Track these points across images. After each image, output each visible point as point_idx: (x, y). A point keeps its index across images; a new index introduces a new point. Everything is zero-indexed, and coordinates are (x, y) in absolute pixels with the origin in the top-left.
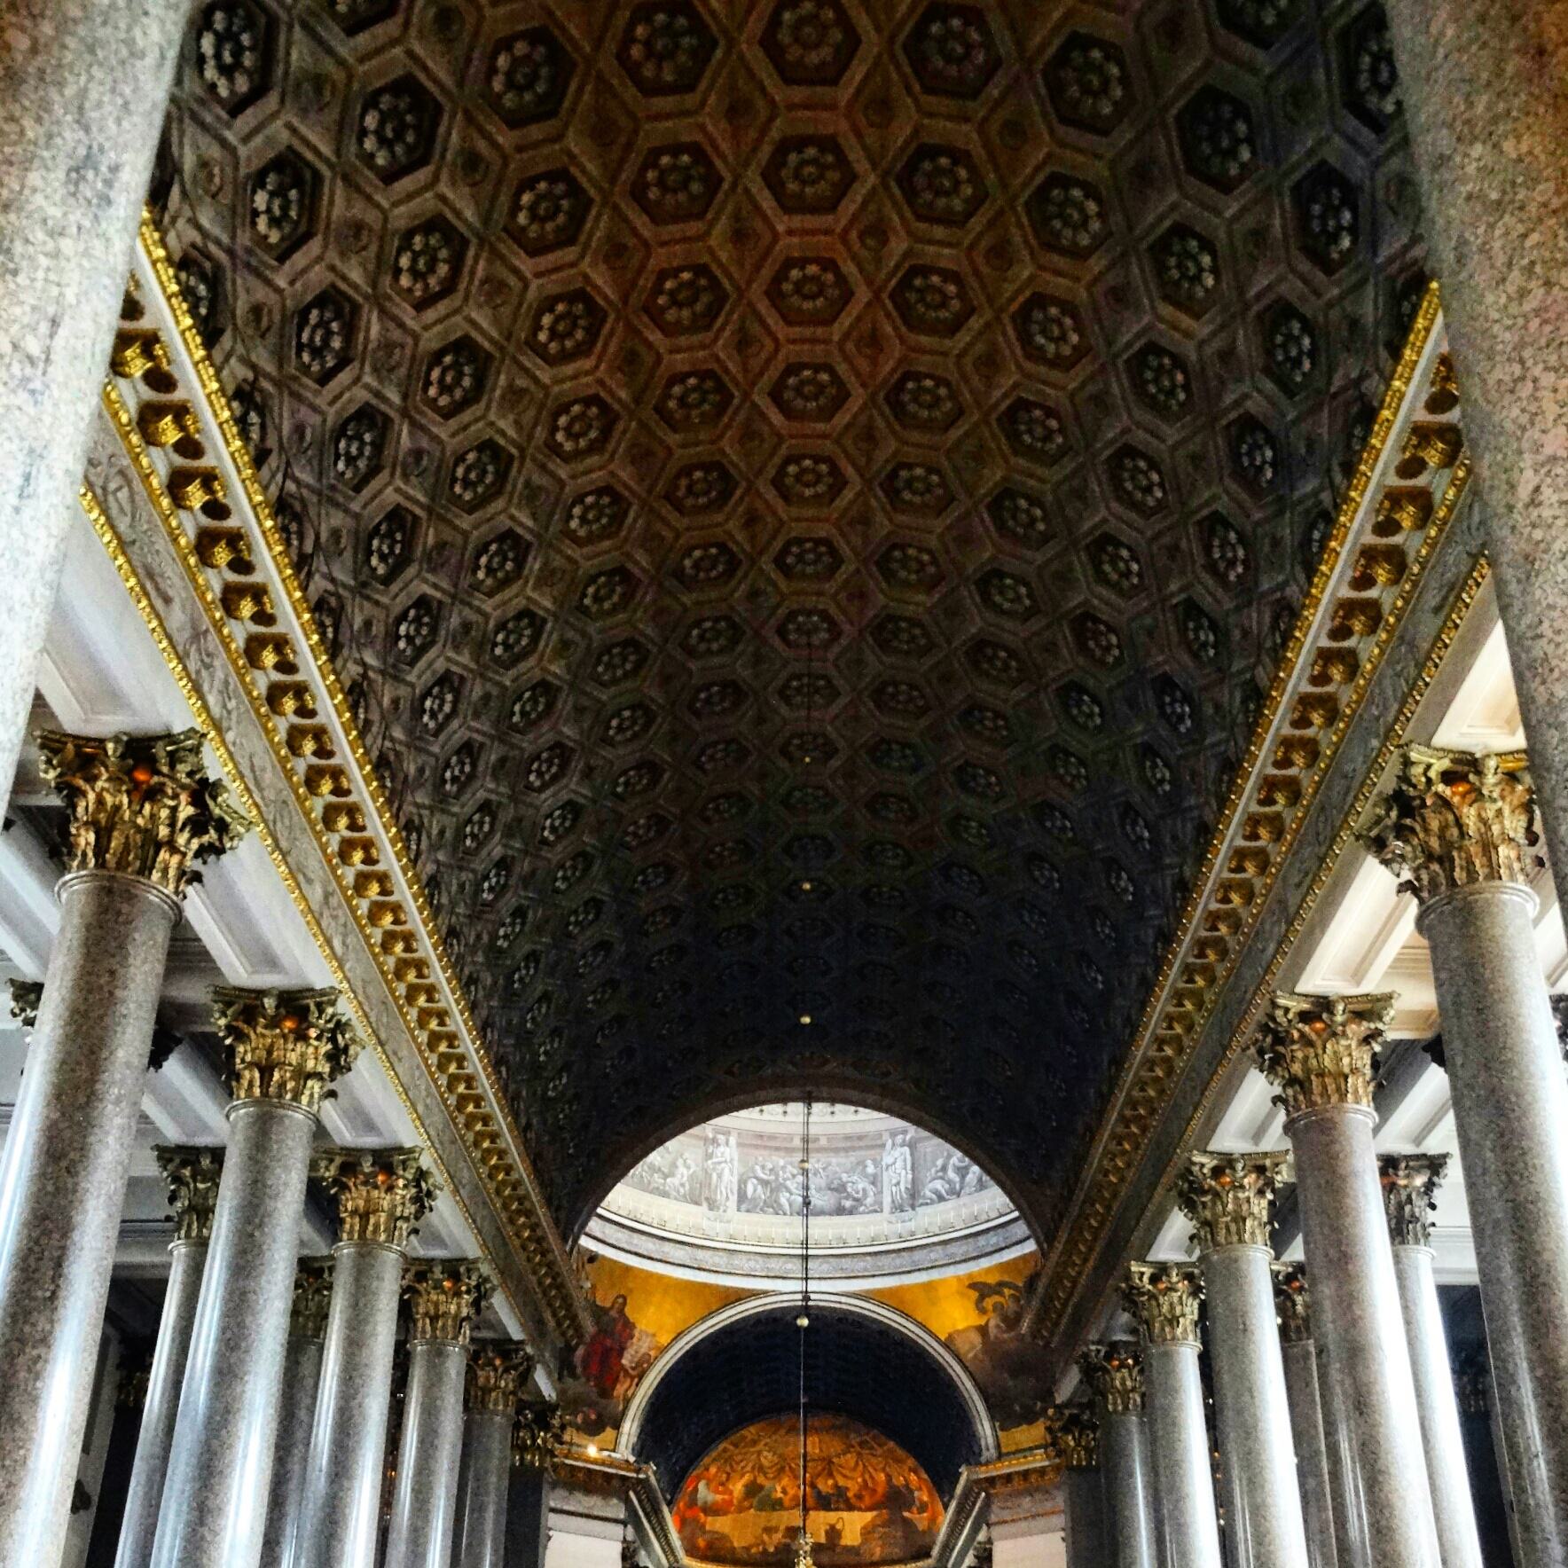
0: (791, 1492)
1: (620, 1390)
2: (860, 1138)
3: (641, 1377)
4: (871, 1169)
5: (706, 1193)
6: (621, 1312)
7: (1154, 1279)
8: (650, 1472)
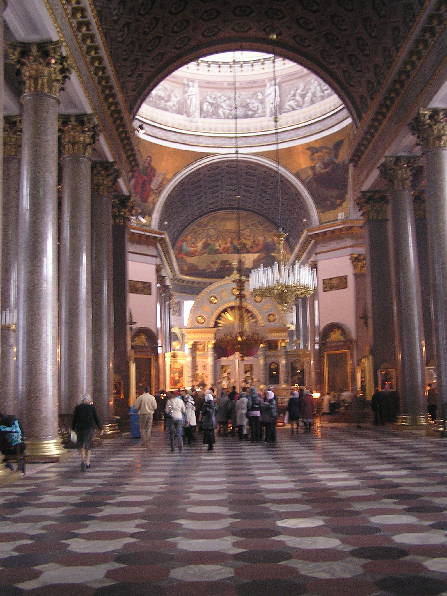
0: (223, 246)
1: (150, 199)
2: (255, 82)
3: (160, 193)
4: (260, 97)
5: (185, 110)
6: (149, 164)
7: (431, 117)
8: (166, 237)
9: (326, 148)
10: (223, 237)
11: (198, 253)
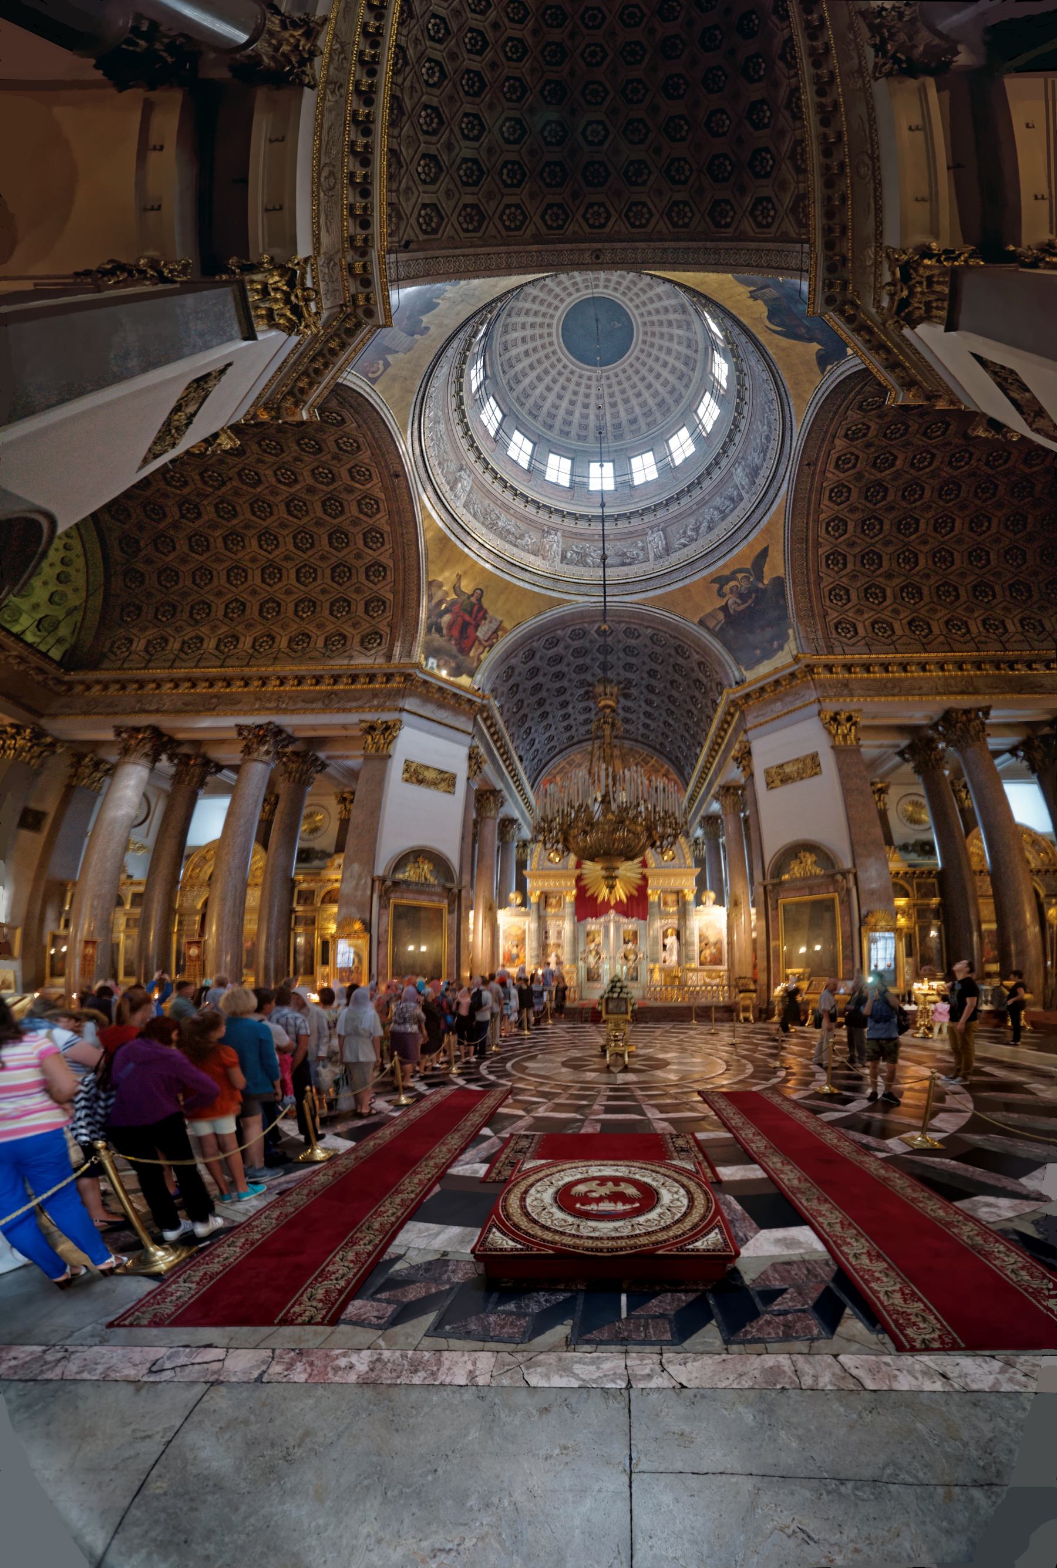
9: (740, 571)
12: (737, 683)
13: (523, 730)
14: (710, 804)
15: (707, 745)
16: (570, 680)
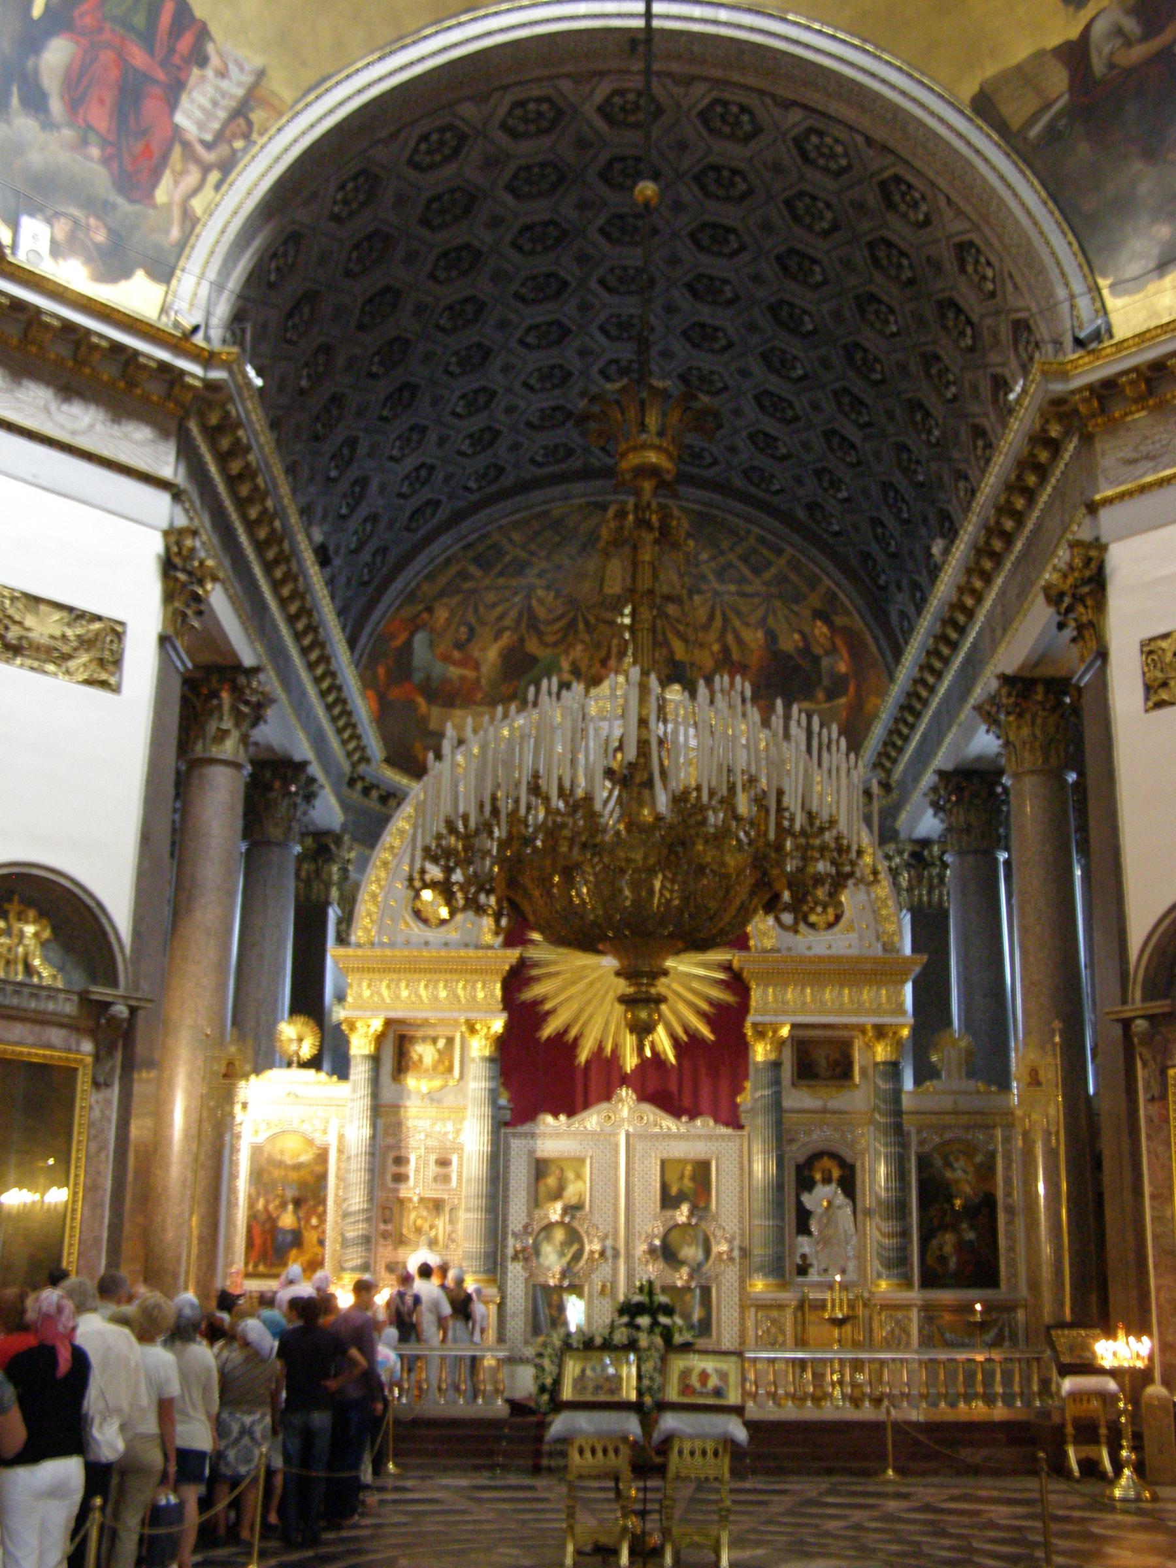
3: (227, 167)
10: (589, 628)
11: (479, 696)
12: (1079, 343)
13: (327, 448)
14: (969, 733)
15: (969, 532)
16: (497, 277)
